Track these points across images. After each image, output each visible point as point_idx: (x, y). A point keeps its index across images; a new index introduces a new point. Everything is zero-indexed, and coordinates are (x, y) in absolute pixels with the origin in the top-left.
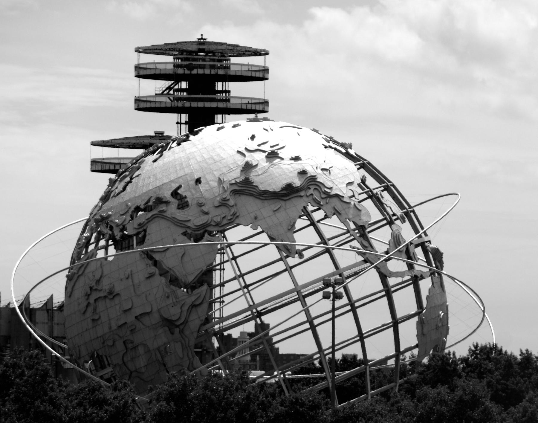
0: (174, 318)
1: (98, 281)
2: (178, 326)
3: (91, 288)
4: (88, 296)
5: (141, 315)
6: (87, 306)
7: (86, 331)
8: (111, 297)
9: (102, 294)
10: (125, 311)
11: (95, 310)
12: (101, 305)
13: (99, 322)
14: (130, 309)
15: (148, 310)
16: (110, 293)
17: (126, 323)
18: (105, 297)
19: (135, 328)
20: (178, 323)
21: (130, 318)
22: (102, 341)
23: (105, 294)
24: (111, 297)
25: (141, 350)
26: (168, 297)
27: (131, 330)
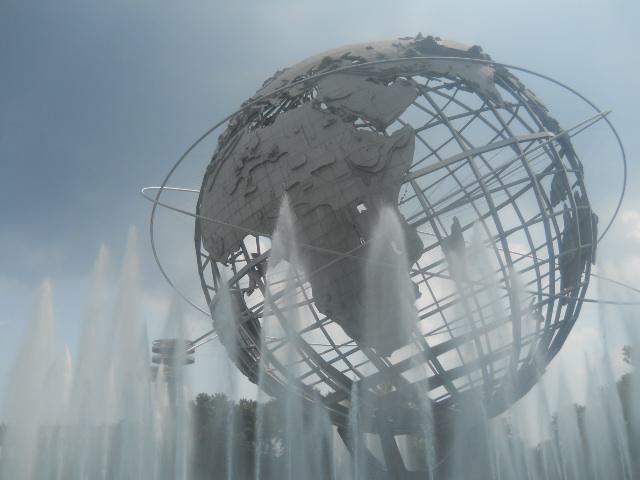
0: (370, 164)
1: (254, 150)
2: (375, 174)
3: (244, 160)
4: (239, 170)
5: (320, 169)
6: (237, 184)
7: (235, 213)
8: (275, 158)
9: (261, 161)
10: (297, 169)
11: (250, 181)
12: (259, 173)
13: (256, 194)
14: (303, 165)
15: (332, 161)
16: (273, 154)
17: (297, 183)
18: (265, 162)
19: (311, 187)
20: (376, 170)
21: (304, 176)
22: (260, 215)
23: (266, 159)
24: (275, 158)
25: (320, 213)
26: (359, 140)
27: (305, 191)
